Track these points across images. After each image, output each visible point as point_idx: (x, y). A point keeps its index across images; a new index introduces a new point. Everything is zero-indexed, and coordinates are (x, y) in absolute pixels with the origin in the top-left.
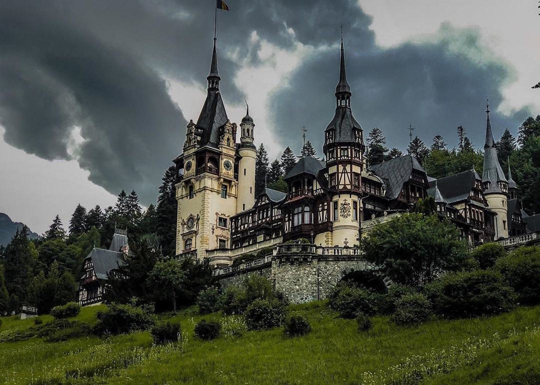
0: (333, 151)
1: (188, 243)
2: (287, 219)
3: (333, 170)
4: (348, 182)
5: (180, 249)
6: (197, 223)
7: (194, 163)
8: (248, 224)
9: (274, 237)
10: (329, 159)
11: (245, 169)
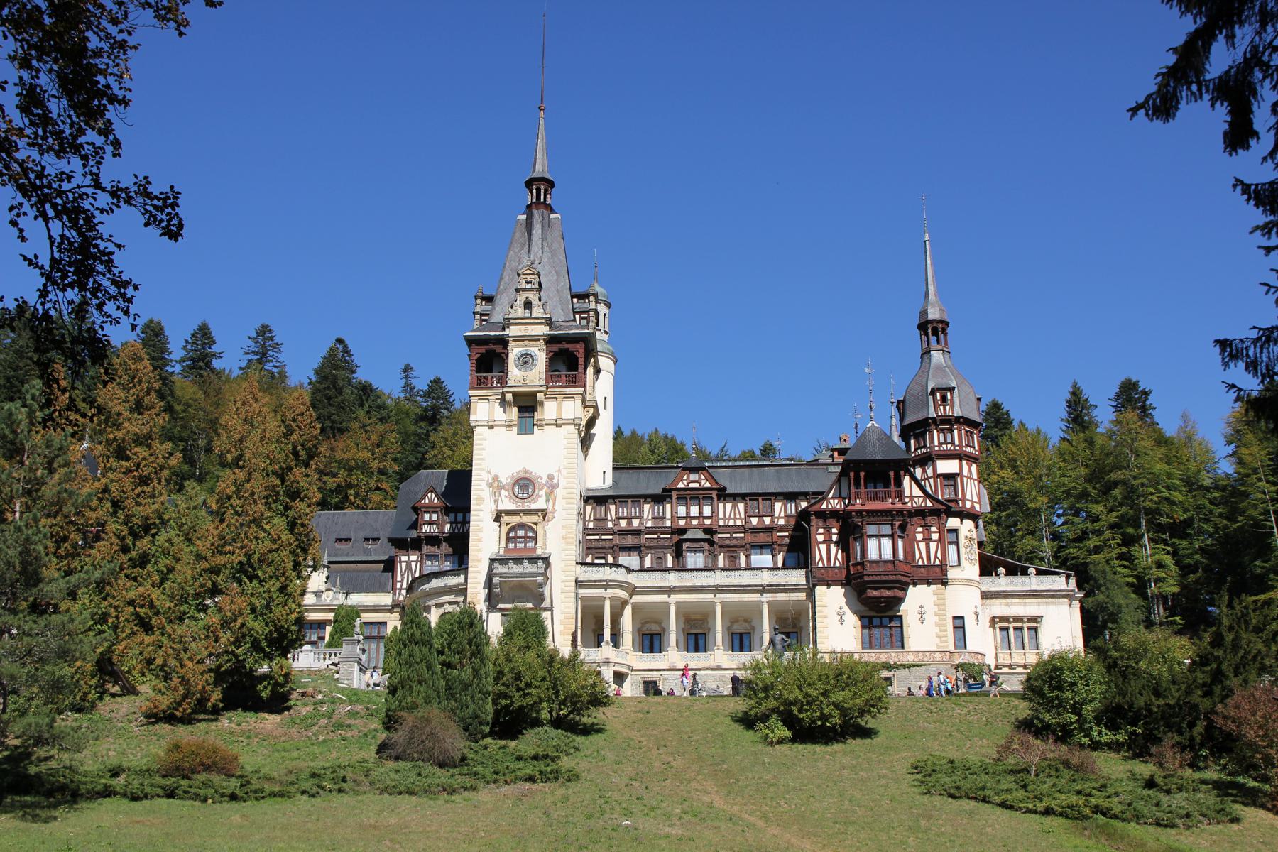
0: (951, 431)
3: (946, 466)
4: (975, 499)
5: (485, 539)
6: (548, 495)
7: (541, 356)
8: (640, 518)
9: (721, 559)
10: (940, 444)
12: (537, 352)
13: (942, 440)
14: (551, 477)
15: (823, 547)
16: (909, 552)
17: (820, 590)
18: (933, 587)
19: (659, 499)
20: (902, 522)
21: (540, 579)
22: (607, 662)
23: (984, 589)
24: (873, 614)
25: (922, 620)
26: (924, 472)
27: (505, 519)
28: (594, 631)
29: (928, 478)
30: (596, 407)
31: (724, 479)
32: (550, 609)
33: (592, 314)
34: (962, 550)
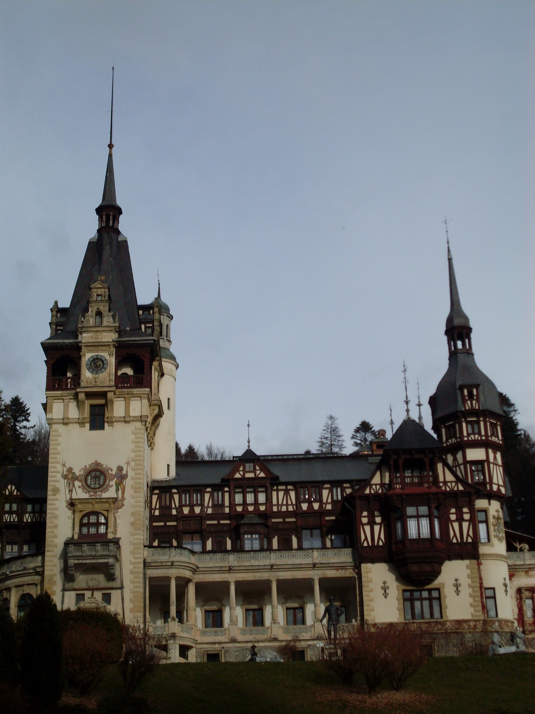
0: (478, 422)
1: (93, 519)
2: (365, 520)
3: (475, 454)
5: (61, 525)
6: (117, 485)
7: (112, 361)
8: (202, 505)
10: (469, 435)
11: (169, 399)
12: (107, 357)
13: (470, 431)
14: (120, 469)
15: (367, 528)
16: (444, 530)
17: (364, 567)
18: (467, 562)
19: (217, 488)
20: (439, 504)
21: (111, 561)
22: (173, 636)
23: (511, 562)
24: (414, 588)
25: (458, 592)
26: (455, 459)
27: (80, 507)
28: (160, 609)
29: (459, 465)
30: (160, 407)
31: (277, 470)
32: (121, 588)
33: (156, 323)
34: (492, 528)
